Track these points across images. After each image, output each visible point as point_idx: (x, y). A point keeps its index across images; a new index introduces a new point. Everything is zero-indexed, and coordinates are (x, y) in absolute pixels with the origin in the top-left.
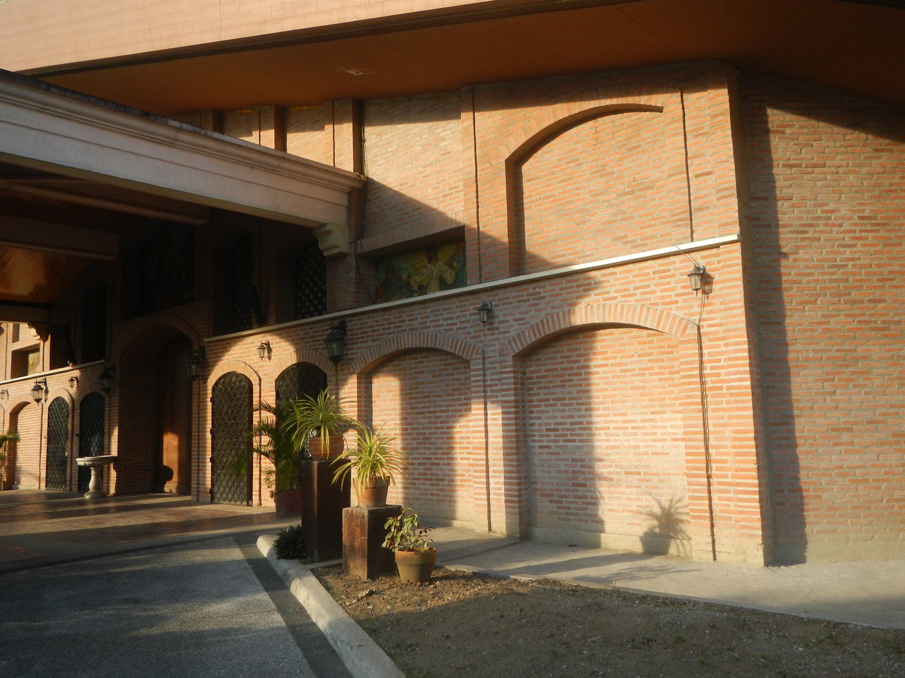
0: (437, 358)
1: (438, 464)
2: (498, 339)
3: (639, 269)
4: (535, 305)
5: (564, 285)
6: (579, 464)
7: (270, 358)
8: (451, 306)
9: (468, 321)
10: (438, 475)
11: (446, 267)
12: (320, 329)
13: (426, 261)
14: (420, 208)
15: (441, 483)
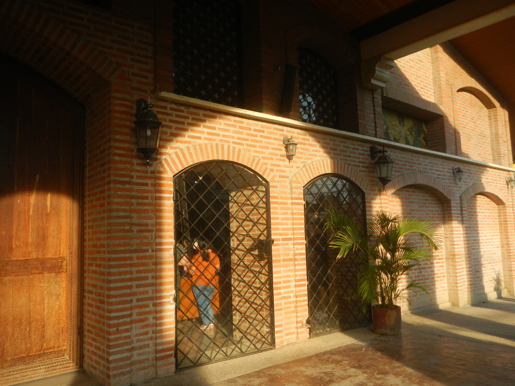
0: (420, 194)
1: (425, 268)
2: (458, 190)
3: (495, 172)
4: (469, 176)
5: (478, 170)
6: (476, 260)
7: (290, 157)
8: (438, 163)
9: (445, 176)
10: (425, 276)
11: (408, 133)
12: (351, 146)
13: (398, 122)
14: (408, 86)
15: (427, 281)
